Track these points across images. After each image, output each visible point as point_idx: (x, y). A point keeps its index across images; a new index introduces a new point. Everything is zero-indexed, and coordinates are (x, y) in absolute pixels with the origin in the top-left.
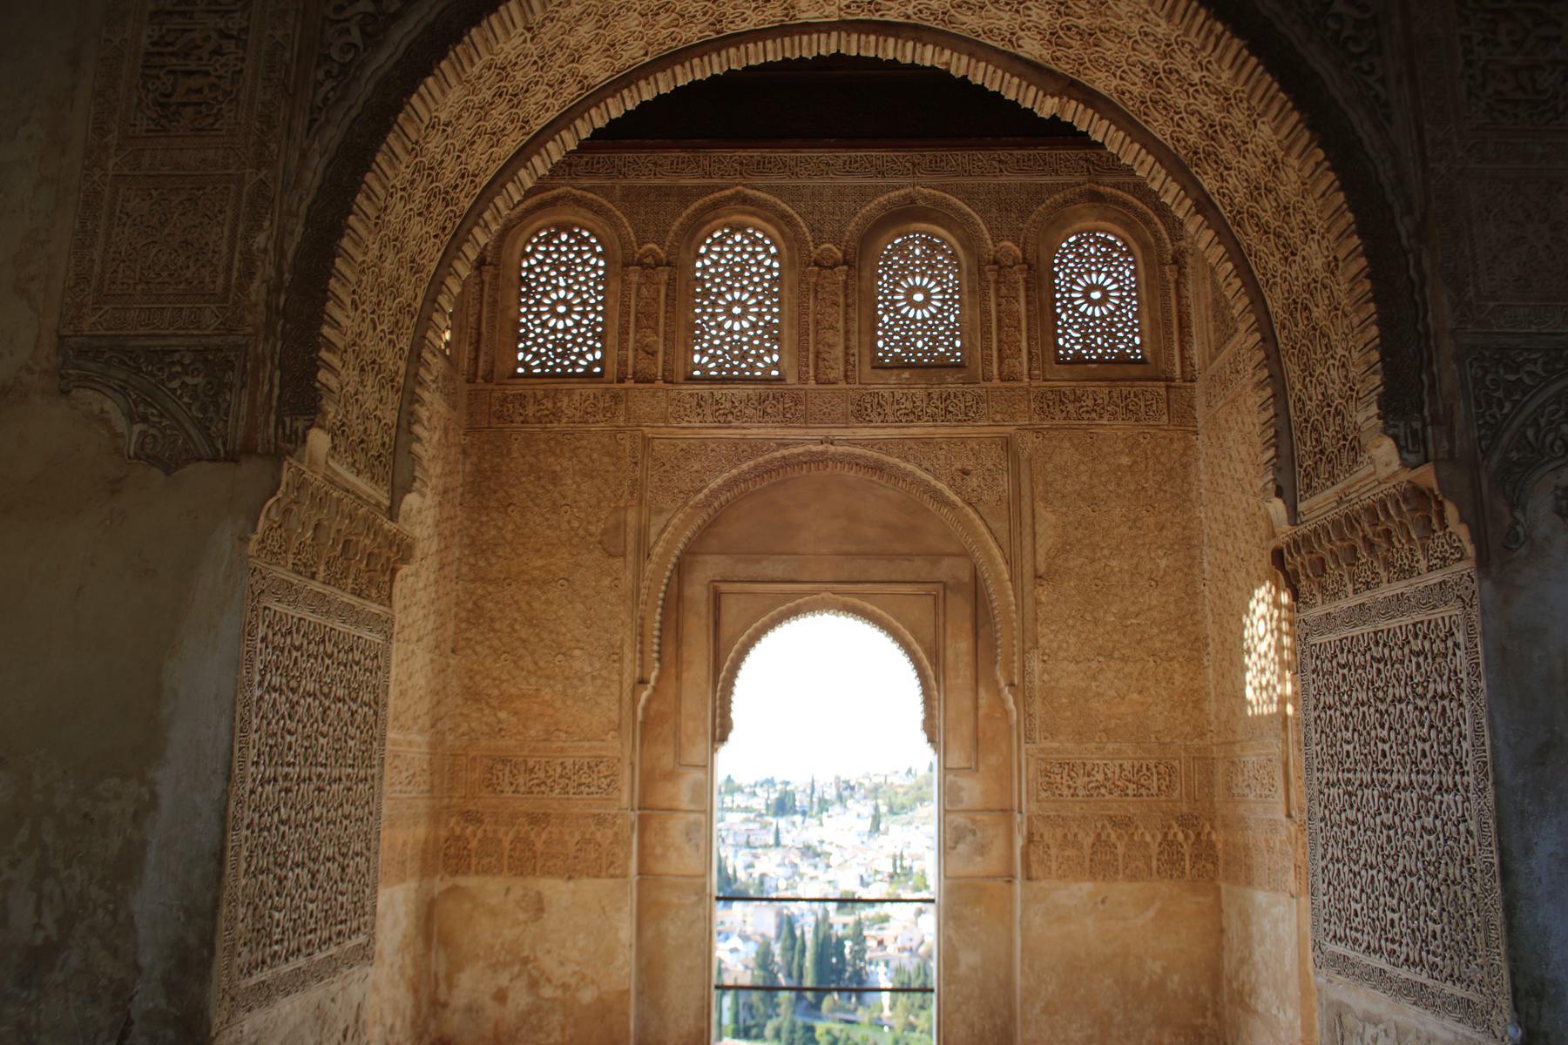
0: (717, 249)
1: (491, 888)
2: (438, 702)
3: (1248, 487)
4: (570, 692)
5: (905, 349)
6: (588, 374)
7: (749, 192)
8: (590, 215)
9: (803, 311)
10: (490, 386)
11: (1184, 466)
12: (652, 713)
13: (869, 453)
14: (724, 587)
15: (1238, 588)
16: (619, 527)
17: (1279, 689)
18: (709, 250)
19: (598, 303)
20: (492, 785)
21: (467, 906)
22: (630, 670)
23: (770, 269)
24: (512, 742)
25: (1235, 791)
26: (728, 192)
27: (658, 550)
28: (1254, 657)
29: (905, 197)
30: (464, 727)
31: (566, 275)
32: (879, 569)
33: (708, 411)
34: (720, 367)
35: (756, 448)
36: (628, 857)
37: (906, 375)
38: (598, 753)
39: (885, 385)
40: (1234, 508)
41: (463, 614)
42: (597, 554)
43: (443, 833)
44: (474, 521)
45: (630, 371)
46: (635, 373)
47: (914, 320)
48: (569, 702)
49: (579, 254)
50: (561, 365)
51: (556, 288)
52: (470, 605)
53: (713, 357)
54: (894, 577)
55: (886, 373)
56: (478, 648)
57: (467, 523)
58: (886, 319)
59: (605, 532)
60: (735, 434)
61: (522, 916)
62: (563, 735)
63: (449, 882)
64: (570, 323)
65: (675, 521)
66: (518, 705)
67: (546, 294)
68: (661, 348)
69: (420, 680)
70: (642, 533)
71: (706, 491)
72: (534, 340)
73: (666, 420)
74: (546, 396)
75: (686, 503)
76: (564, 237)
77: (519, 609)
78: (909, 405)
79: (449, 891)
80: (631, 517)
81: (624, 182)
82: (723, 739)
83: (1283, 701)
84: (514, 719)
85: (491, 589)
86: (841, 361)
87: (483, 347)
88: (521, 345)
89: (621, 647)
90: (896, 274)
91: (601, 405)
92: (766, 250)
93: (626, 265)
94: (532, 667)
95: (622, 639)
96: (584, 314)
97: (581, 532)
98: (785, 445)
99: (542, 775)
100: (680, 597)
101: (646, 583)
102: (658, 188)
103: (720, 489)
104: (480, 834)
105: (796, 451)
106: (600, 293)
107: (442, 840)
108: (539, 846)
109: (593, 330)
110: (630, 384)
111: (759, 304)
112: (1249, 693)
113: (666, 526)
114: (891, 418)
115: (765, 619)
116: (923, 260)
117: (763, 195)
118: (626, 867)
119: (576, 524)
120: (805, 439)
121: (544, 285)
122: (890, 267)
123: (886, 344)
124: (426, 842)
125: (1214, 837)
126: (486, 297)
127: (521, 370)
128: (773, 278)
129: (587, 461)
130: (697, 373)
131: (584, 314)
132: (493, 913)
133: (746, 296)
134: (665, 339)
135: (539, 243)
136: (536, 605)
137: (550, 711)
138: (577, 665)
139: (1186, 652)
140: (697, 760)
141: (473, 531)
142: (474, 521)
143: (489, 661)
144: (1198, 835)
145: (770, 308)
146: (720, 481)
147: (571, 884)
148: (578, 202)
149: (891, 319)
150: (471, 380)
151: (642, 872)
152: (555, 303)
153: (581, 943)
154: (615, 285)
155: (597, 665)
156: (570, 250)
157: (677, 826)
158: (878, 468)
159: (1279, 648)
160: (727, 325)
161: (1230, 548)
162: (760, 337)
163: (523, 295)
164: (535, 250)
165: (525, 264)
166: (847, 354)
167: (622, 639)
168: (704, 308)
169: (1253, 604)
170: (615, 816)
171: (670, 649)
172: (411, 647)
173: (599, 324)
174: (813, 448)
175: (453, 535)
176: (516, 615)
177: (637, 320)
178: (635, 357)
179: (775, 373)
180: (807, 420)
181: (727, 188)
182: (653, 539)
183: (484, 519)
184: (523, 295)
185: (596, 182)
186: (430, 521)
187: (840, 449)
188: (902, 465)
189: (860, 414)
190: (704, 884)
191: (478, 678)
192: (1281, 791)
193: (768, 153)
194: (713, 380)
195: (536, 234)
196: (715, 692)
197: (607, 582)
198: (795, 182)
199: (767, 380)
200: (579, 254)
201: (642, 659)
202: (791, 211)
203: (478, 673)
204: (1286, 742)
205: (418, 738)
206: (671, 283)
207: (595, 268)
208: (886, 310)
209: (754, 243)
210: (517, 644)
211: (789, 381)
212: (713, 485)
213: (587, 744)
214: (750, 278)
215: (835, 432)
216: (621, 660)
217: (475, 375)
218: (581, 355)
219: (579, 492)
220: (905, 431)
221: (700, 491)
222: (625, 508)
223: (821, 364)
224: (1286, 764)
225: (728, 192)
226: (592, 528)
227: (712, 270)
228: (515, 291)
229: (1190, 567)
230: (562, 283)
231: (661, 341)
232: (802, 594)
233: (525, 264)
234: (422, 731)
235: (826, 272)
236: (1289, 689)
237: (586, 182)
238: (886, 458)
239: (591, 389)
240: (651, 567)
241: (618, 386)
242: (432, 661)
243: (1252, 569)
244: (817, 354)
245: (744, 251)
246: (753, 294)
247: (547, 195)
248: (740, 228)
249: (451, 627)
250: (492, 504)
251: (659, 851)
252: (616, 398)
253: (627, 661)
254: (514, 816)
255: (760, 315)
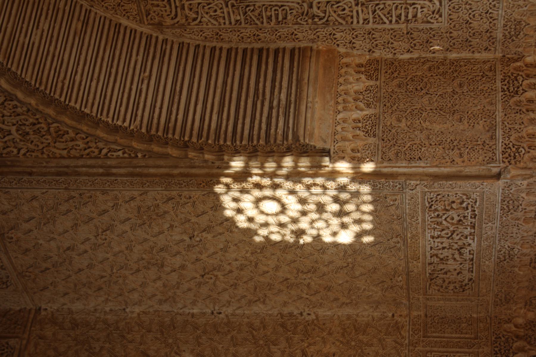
3: (105, 218)
11: (75, 325)
15: (225, 250)
17: (343, 180)
25: (467, 275)
28: (304, 224)
40: (129, 248)
83: (359, 177)
112: (346, 237)
125: (520, 321)
139: (297, 338)
144: (517, 337)
159: (295, 176)
161: (178, 261)
169: (241, 222)
192: (466, 186)
204: (410, 176)
224: (436, 177)
229: (196, 328)
236: (343, 166)
243: (204, 221)
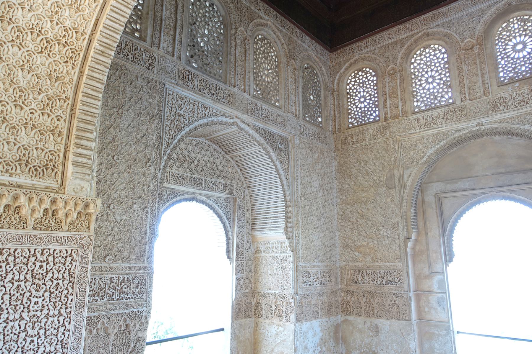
0: (419, 58)
1: (359, 321)
2: (330, 250)
4: (380, 243)
5: (516, 73)
6: (375, 121)
7: (430, 30)
8: (368, 63)
9: (460, 71)
10: (340, 134)
12: (417, 250)
13: (502, 126)
14: (443, 195)
16: (392, 176)
18: (416, 60)
19: (375, 94)
20: (355, 281)
21: (351, 328)
22: (403, 234)
23: (443, 59)
24: (361, 264)
26: (420, 34)
27: (409, 184)
29: (505, 5)
30: (344, 259)
31: (363, 87)
32: (518, 178)
33: (422, 124)
34: (426, 105)
35: (445, 135)
36: (410, 311)
37: (517, 84)
38: (393, 268)
39: (507, 92)
41: (340, 217)
42: (384, 189)
43: (340, 298)
44: (340, 183)
45: (389, 116)
46: (391, 116)
47: (518, 59)
48: (380, 248)
49: (366, 78)
50: (364, 120)
51: (360, 93)
52: (341, 213)
53: (423, 102)
54: (528, 181)
55: (506, 87)
56: (346, 229)
57: (338, 184)
58: (503, 62)
59: (386, 180)
60: (436, 131)
61: (371, 334)
62: (379, 261)
63: (344, 317)
64: (366, 104)
65: (415, 171)
66: (362, 249)
67: (356, 96)
68: (400, 104)
69: (319, 243)
70: (401, 178)
71: (426, 157)
72: (354, 113)
73: (405, 132)
74: (359, 133)
75: (418, 163)
76: (360, 73)
77: (358, 213)
78: (521, 98)
79: (344, 321)
80: (396, 172)
81: (379, 46)
82: (451, 260)
84: (360, 255)
85: (348, 207)
86: (481, 88)
87: (337, 121)
88: (350, 117)
89: (398, 224)
90: (505, 39)
91: (380, 131)
92: (440, 51)
93: (383, 76)
94: (365, 235)
95: (398, 221)
96: (370, 99)
97: (378, 181)
98: (459, 131)
99: (373, 277)
100: (423, 202)
101: (406, 198)
102: (392, 43)
103: (432, 155)
104: (353, 299)
105: (465, 132)
106: (375, 90)
107: (340, 302)
108: (375, 306)
109: (375, 105)
110: (390, 121)
111: (440, 74)
113: (411, 174)
114: (511, 107)
115: (464, 207)
116: (519, 29)
117: (436, 30)
118: (410, 316)
119: (375, 178)
120: (468, 126)
121: (355, 93)
122: (502, 38)
123: (504, 73)
124: (330, 302)
126: (336, 103)
127: (351, 126)
128: (445, 62)
129: (377, 154)
130: (416, 110)
131: (370, 99)
132: (360, 331)
133: (433, 73)
134: (401, 99)
135: (352, 79)
136: (364, 211)
137: (373, 251)
138: (381, 233)
140: (439, 270)
141: (340, 187)
142: (340, 183)
143: (350, 233)
145: (445, 75)
146: (432, 151)
147: (389, 322)
148: (363, 59)
149: (505, 62)
150: (334, 132)
151: (420, 318)
152: (360, 98)
153: (395, 348)
154: (380, 85)
155: (389, 232)
156: (363, 77)
157: (433, 299)
158: (508, 133)
160: (427, 87)
162: (442, 88)
163: (348, 98)
164: (351, 81)
165: (348, 87)
166: (483, 84)
167: (398, 221)
168: (416, 83)
170: (403, 294)
171: (421, 224)
172: (311, 232)
173: (376, 101)
174: (473, 129)
175: (332, 189)
176: (358, 215)
177: (390, 95)
178: (391, 110)
179: (451, 101)
180: (467, 118)
181: (419, 32)
182: (406, 179)
183: (343, 181)
184: (348, 98)
185: (369, 49)
186: (317, 186)
187: (487, 127)
188: (522, 127)
189: (495, 108)
190: (449, 326)
191: (347, 240)
193: (435, 12)
194: (423, 111)
195: (351, 76)
196: (444, 240)
197: (389, 199)
198: (449, 19)
199: (447, 105)
200: (366, 78)
201: (407, 229)
202: (449, 31)
203: (347, 238)
205: (320, 264)
206: (402, 76)
207: (373, 81)
208: (502, 58)
209: (434, 51)
210: (359, 226)
211: (457, 103)
212: (429, 154)
213: (388, 264)
214: (435, 65)
215: (483, 120)
216: (398, 230)
217: (335, 131)
218: (371, 115)
219: (375, 166)
220: (521, 111)
221: (423, 157)
222: (393, 169)
223: (471, 92)
225: (420, 34)
226: (382, 179)
227: (418, 67)
228: (345, 99)
230: (362, 90)
231: (400, 101)
232: (480, 194)
233: (348, 87)
234: (321, 261)
235: (469, 51)
237: (365, 51)
238: (512, 126)
239: (375, 126)
240: (406, 191)
241: (385, 123)
242: (324, 235)
244: (469, 88)
245: (430, 55)
246: (437, 71)
247: (352, 61)
248: (428, 47)
249: (336, 222)
250: (345, 175)
251: (426, 309)
252: (385, 127)
253: (401, 230)
254: (364, 293)
255: (441, 79)
